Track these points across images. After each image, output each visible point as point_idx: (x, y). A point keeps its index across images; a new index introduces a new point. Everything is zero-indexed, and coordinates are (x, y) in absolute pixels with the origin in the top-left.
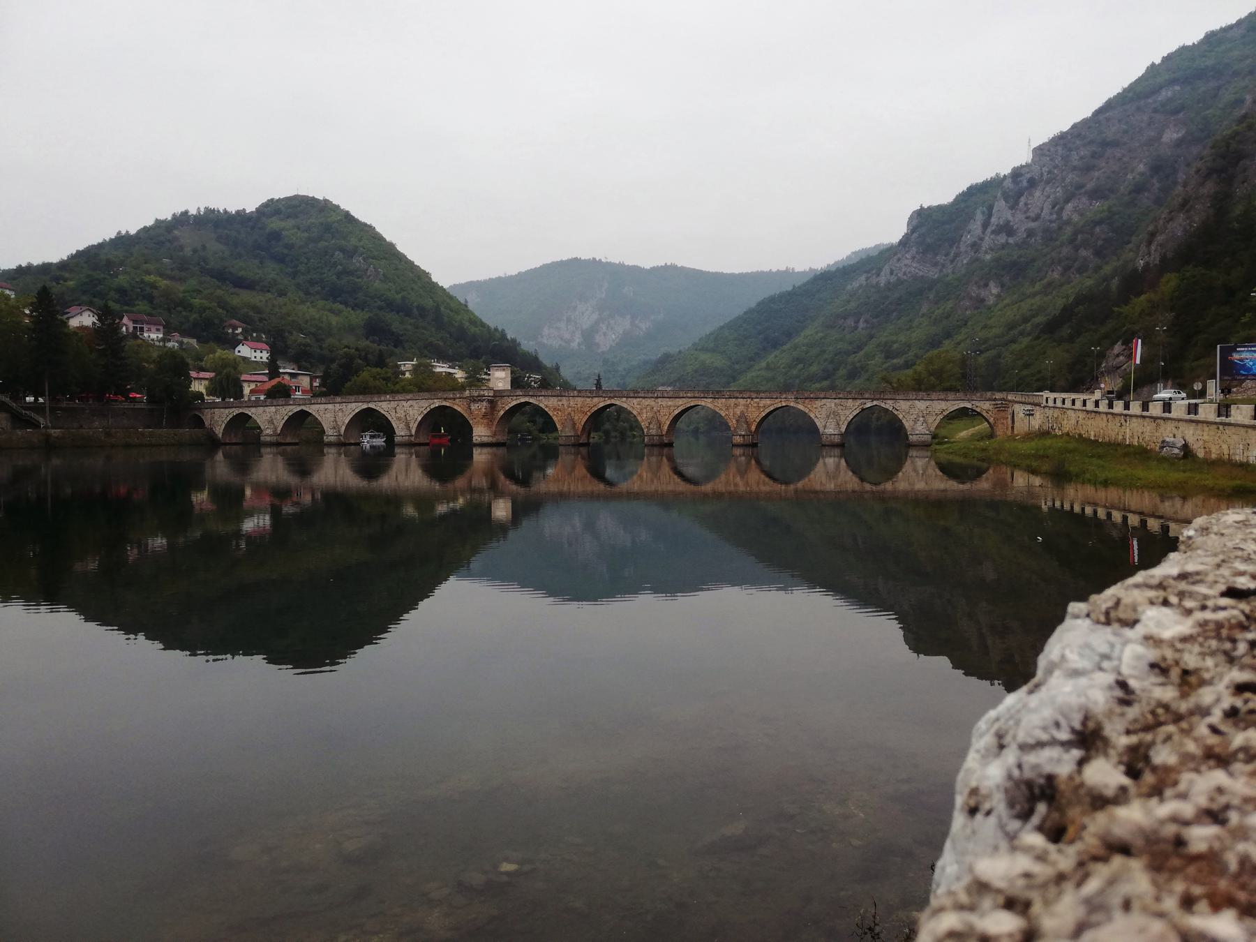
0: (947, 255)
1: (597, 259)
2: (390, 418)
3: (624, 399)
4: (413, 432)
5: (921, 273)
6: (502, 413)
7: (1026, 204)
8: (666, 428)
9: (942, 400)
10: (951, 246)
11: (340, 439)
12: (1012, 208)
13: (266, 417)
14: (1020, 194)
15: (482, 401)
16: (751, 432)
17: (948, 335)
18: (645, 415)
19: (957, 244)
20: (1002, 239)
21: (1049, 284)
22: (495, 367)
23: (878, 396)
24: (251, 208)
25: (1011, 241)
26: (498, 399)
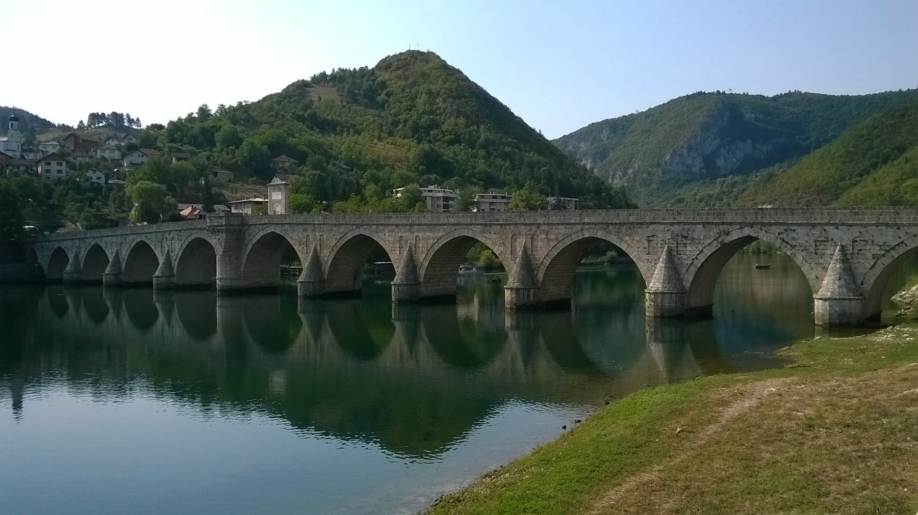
1: (721, 92)
3: (374, 227)
6: (250, 247)
8: (422, 272)
9: (887, 225)
15: (223, 233)
18: (398, 252)
23: (750, 219)
24: (371, 65)
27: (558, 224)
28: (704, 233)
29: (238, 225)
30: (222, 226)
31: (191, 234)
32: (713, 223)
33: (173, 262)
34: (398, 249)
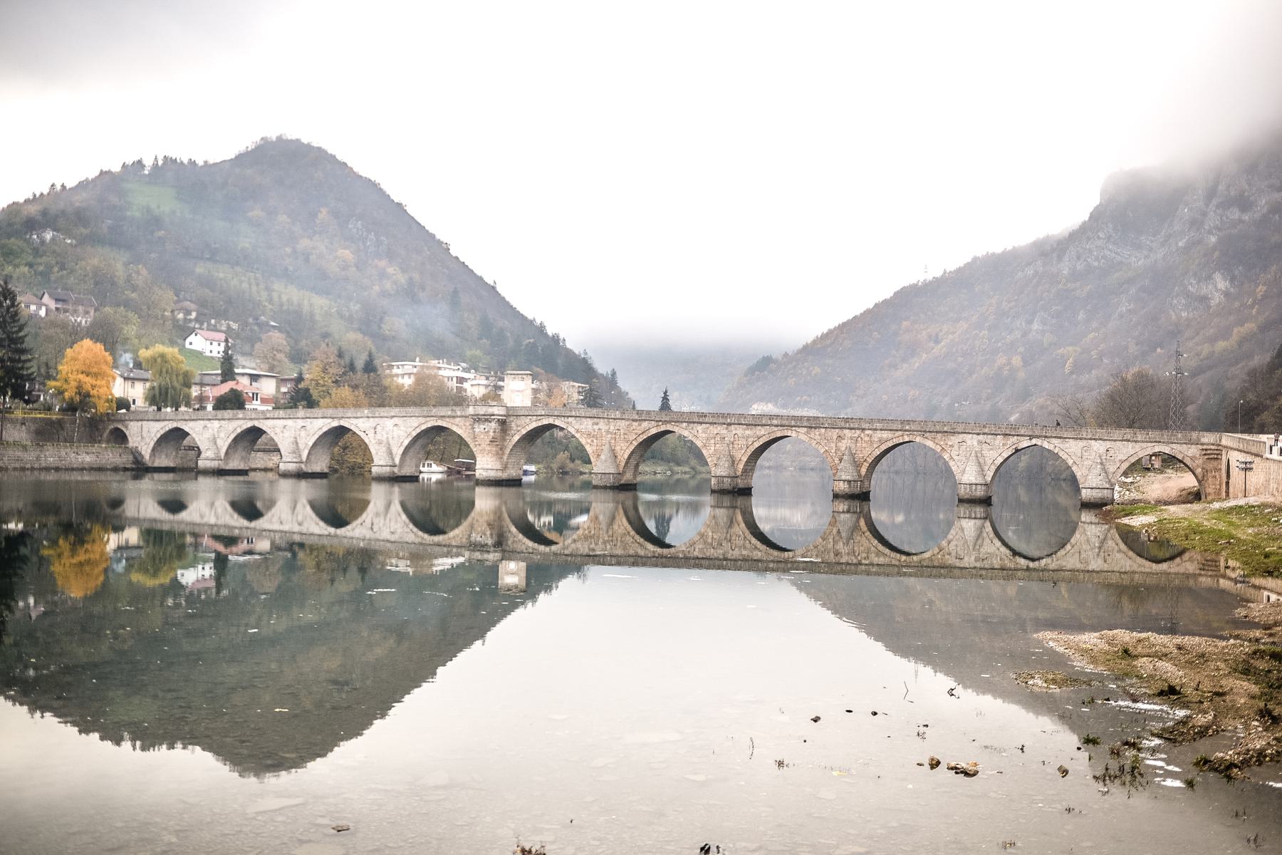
2: (367, 441)
3: (685, 424)
4: (397, 461)
5: (1119, 258)
6: (516, 438)
8: (741, 466)
9: (1129, 441)
11: (300, 466)
13: (208, 434)
15: (490, 422)
16: (860, 476)
18: (713, 448)
22: (511, 374)
26: (512, 419)
27: (881, 430)
28: (1002, 442)
29: (504, 416)
30: (493, 415)
31: (426, 422)
32: (1010, 435)
33: (394, 451)
34: (713, 445)
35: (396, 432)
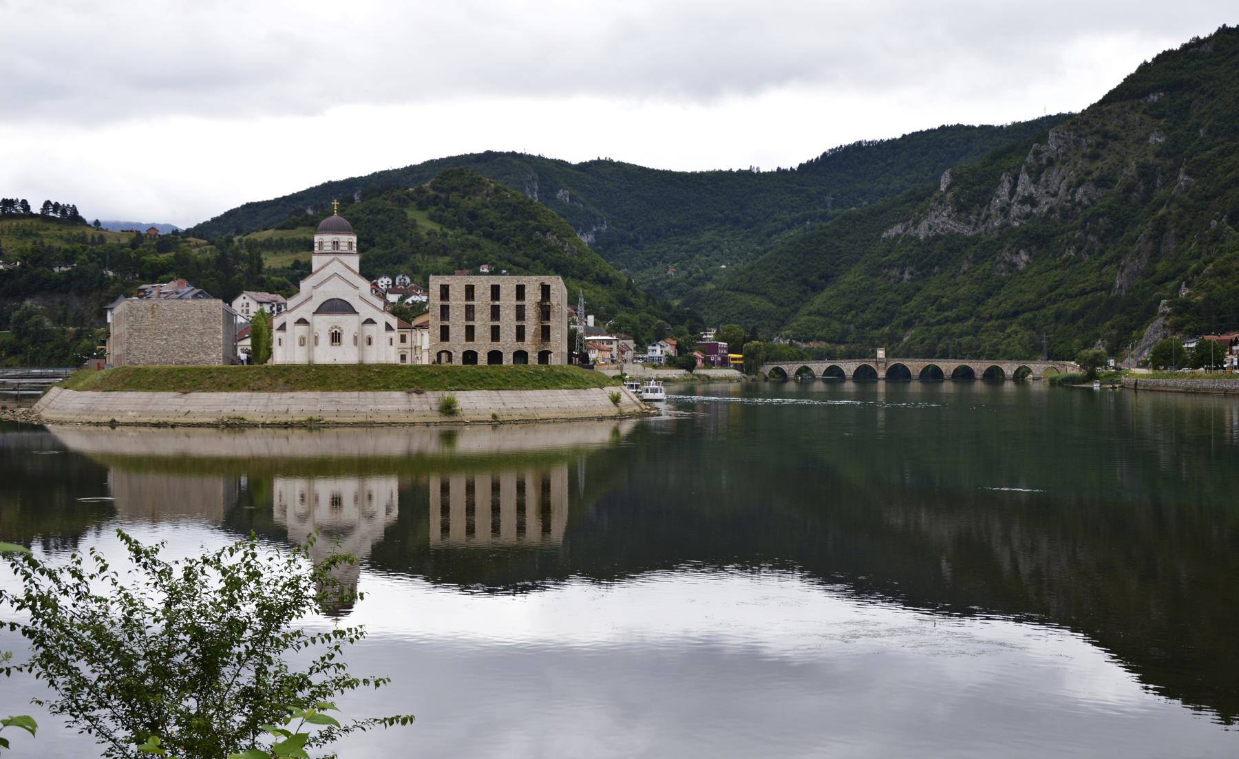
0: (979, 215)
5: (956, 231)
7: (1046, 181)
10: (982, 207)
12: (1035, 182)
14: (1040, 172)
17: (989, 295)
19: (987, 206)
20: (1027, 208)
21: (1066, 260)
25: (1035, 211)
35: (851, 366)
